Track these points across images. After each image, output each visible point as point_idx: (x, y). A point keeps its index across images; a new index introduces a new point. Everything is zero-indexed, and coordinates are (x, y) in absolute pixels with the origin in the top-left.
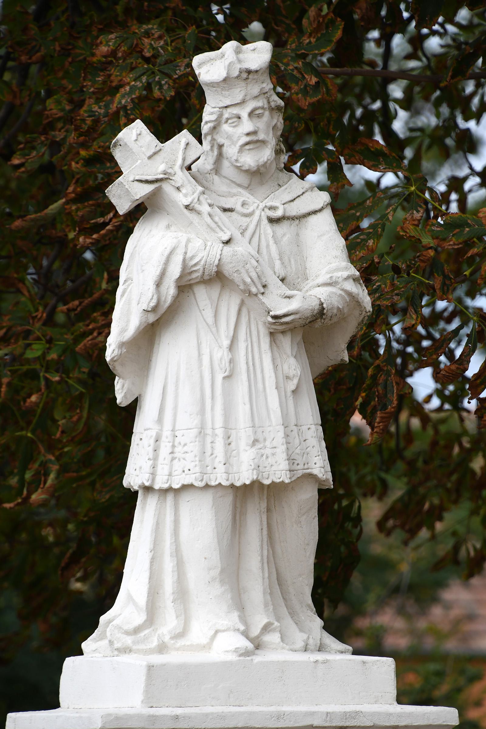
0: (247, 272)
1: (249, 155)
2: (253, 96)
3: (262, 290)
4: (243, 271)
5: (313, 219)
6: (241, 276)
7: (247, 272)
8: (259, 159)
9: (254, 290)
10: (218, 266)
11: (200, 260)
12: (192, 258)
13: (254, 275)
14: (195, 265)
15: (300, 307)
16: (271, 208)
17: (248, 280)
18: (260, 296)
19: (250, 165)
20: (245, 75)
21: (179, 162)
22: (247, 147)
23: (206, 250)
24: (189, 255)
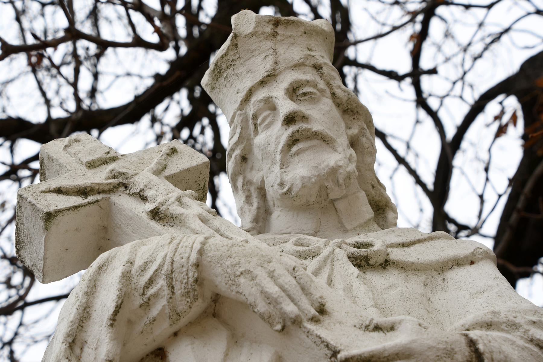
0: (272, 275)
1: (300, 164)
2: (292, 63)
3: (313, 312)
4: (261, 274)
5: (457, 275)
6: (257, 285)
7: (272, 275)
8: (320, 164)
9: (290, 308)
10: (197, 265)
11: (160, 267)
12: (144, 268)
13: (288, 280)
14: (151, 282)
15: (414, 341)
16: (358, 246)
17: (273, 289)
18: (310, 326)
19: (303, 178)
20: (269, 29)
21: (153, 165)
22: (294, 149)
23: (172, 245)
24: (139, 262)
